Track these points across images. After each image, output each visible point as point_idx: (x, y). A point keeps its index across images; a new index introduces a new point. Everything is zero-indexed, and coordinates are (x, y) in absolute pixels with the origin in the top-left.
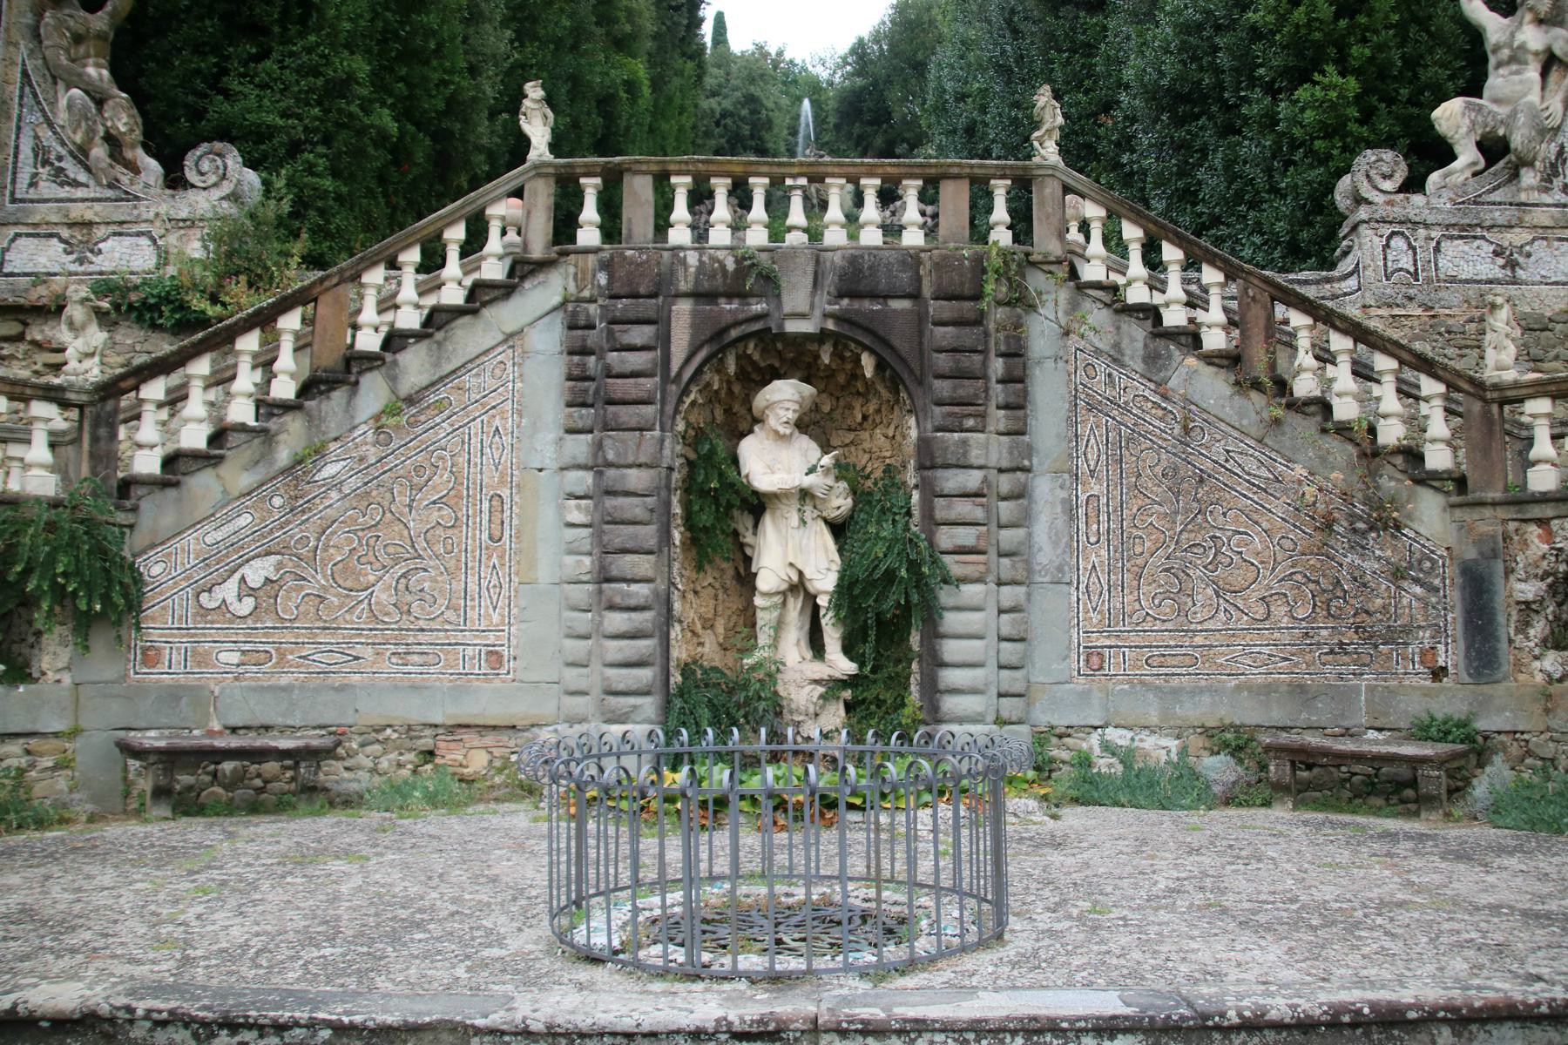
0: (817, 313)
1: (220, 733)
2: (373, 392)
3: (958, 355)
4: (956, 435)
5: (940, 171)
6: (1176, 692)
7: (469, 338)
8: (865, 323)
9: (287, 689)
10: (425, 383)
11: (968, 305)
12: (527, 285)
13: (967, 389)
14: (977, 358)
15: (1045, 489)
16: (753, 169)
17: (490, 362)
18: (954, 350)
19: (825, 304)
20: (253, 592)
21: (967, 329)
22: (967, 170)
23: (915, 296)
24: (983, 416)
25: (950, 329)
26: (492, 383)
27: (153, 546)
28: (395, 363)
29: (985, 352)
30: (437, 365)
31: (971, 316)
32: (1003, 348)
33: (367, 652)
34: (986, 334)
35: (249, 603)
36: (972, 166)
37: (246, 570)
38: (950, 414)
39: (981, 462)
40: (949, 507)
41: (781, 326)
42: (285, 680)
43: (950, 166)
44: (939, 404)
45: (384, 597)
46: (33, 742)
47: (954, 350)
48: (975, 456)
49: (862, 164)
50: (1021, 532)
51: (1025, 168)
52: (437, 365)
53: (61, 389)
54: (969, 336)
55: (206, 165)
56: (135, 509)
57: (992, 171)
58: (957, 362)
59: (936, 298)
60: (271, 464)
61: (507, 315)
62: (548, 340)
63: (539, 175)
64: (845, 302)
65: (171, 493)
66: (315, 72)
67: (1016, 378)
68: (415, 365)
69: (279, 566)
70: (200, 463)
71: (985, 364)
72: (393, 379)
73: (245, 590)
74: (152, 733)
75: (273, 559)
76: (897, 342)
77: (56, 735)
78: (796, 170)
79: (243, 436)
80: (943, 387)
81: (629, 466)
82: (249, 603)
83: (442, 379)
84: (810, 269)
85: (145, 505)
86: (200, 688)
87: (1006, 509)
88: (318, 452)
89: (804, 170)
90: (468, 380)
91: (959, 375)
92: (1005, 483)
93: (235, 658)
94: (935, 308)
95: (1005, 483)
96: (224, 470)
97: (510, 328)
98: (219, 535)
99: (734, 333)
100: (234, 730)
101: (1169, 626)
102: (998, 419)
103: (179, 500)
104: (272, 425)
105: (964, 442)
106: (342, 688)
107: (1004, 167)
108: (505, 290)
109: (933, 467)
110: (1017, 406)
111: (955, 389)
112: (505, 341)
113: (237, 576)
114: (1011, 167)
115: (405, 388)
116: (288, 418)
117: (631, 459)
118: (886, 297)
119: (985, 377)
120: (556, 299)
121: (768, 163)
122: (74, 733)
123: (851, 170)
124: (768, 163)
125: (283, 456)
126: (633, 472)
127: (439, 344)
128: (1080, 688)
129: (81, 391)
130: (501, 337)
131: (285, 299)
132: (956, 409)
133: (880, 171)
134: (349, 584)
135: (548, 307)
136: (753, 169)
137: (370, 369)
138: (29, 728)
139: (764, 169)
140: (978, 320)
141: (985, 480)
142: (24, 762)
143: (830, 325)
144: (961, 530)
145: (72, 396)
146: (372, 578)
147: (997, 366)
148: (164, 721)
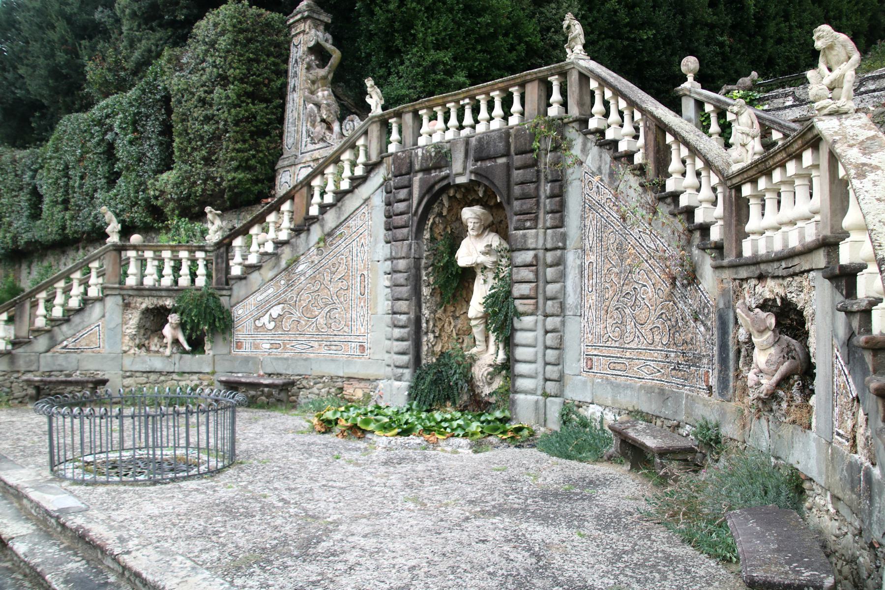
0: (468, 172)
1: (263, 376)
2: (316, 232)
3: (524, 186)
4: (521, 232)
5: (522, 79)
6: (618, 386)
7: (351, 203)
8: (484, 174)
9: (287, 359)
10: (333, 227)
11: (529, 155)
12: (372, 175)
13: (529, 203)
14: (532, 186)
15: (571, 258)
16: (446, 100)
17: (359, 213)
18: (522, 183)
19: (471, 167)
20: (274, 319)
21: (528, 170)
22: (534, 76)
23: (507, 154)
24: (536, 219)
25: (521, 171)
26: (361, 223)
27: (238, 303)
28: (323, 219)
29: (538, 181)
30: (339, 218)
31: (530, 162)
32: (550, 178)
33: (316, 344)
34: (538, 171)
35: (273, 324)
36: (536, 73)
37: (272, 311)
38: (519, 220)
39: (533, 246)
40: (518, 273)
41: (454, 181)
42: (286, 355)
43: (526, 75)
44: (516, 215)
45: (321, 321)
46: (201, 375)
47: (522, 183)
48: (531, 243)
49: (488, 86)
50: (557, 286)
51: (560, 67)
52: (339, 218)
53: (203, 246)
54: (530, 173)
55: (348, 127)
56: (231, 289)
57: (546, 73)
58: (523, 190)
59: (516, 154)
60: (279, 267)
61: (365, 191)
62: (378, 201)
63: (373, 122)
64: (479, 163)
65: (244, 282)
66: (419, 65)
67: (559, 195)
68: (331, 219)
69: (283, 308)
70: (253, 269)
71: (537, 189)
72: (322, 226)
73: (272, 319)
74: (240, 375)
75: (281, 306)
76: (496, 182)
77: (208, 373)
78: (462, 96)
79: (267, 257)
80: (517, 205)
81: (400, 258)
82: (273, 324)
83: (341, 224)
84: (463, 149)
85: (235, 287)
86: (256, 358)
87: (550, 272)
88: (295, 261)
89: (465, 95)
90: (351, 223)
91: (524, 197)
92: (550, 257)
93: (268, 346)
94: (518, 160)
95: (550, 257)
96: (263, 271)
97: (365, 196)
98: (261, 297)
99: (437, 187)
100: (270, 375)
101: (617, 344)
102: (549, 220)
103: (246, 284)
104: (279, 251)
105: (524, 235)
106: (306, 360)
107: (550, 70)
108: (364, 179)
109: (513, 251)
110: (560, 210)
111: (522, 205)
112: (364, 203)
113: (269, 313)
114: (554, 68)
115: (327, 229)
116: (284, 248)
117: (399, 256)
118: (495, 158)
119: (537, 196)
120: (382, 180)
121: (452, 95)
122: (213, 373)
123: (484, 90)
124: (452, 95)
125: (283, 264)
126: (401, 261)
127: (340, 208)
128: (583, 379)
129: (210, 246)
130: (362, 201)
131: (281, 198)
132: (521, 217)
133: (496, 87)
134: (308, 316)
135: (378, 184)
136: (446, 100)
137: (314, 223)
138: (199, 370)
139: (450, 99)
140: (535, 163)
141: (536, 256)
142: (198, 382)
143: (473, 178)
144: (524, 286)
145: (207, 248)
146: (317, 313)
147: (546, 188)
148: (243, 370)
